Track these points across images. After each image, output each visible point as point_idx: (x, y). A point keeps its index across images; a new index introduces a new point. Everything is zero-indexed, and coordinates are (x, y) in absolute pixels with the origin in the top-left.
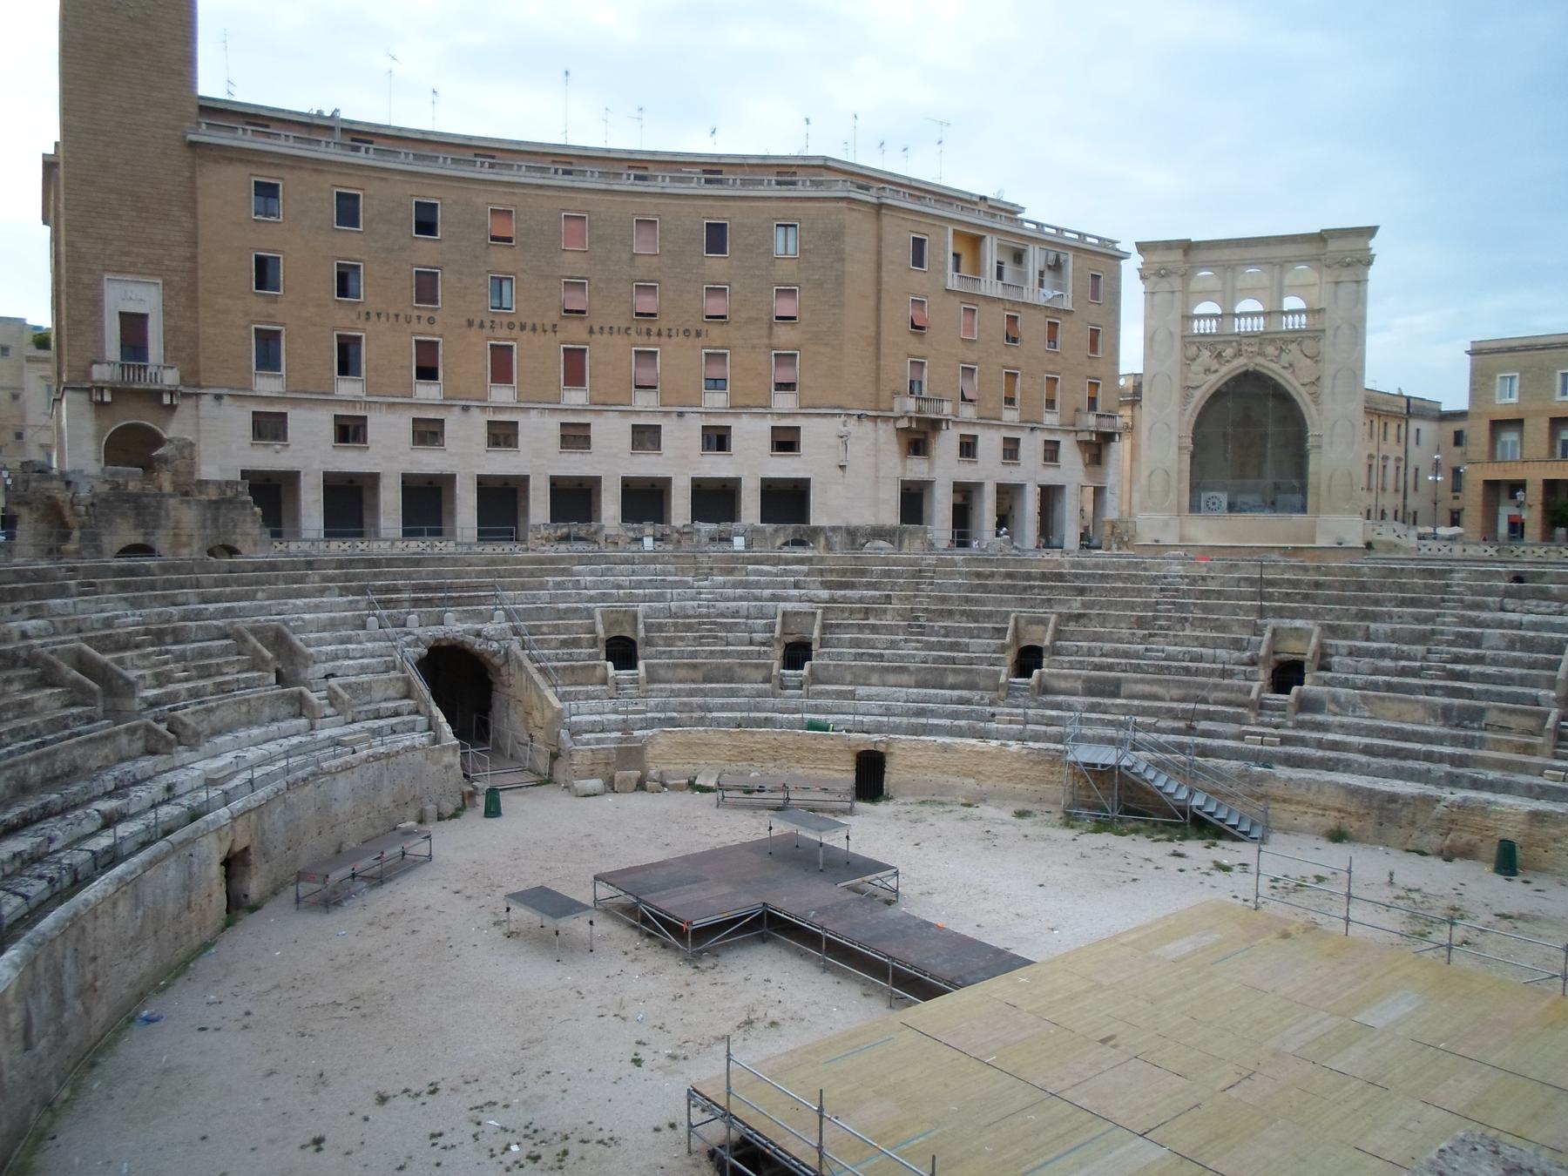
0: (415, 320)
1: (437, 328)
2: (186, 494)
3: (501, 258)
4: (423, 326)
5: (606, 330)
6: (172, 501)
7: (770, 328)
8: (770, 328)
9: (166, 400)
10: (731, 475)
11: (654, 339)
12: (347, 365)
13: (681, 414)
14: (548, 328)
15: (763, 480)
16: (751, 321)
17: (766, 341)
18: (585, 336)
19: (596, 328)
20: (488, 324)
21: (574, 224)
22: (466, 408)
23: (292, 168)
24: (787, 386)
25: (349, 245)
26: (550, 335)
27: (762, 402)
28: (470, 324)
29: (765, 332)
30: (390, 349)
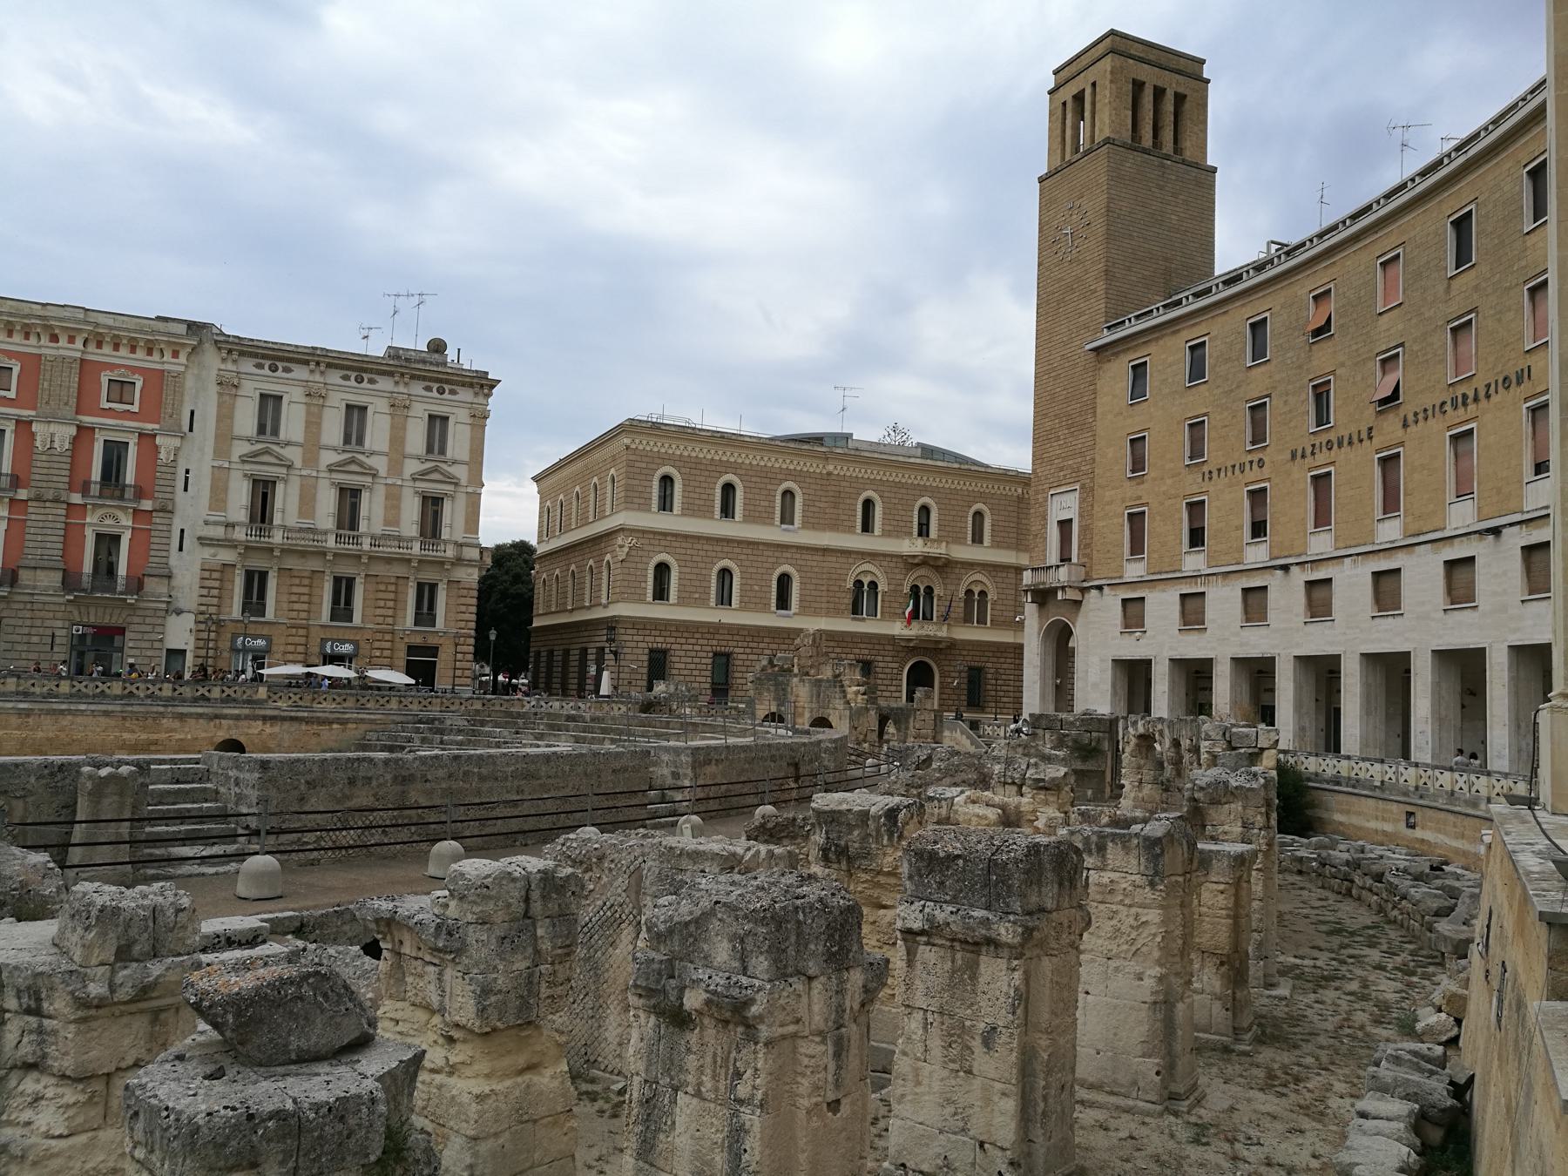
2: (807, 674)
3: (1324, 358)
5: (1421, 416)
6: (795, 680)
9: (1060, 594)
11: (1472, 407)
12: (1197, 537)
13: (1496, 531)
18: (1400, 432)
19: (1411, 418)
21: (1391, 270)
22: (1285, 568)
23: (1157, 339)
25: (1199, 401)
26: (1366, 443)
30: (1227, 510)
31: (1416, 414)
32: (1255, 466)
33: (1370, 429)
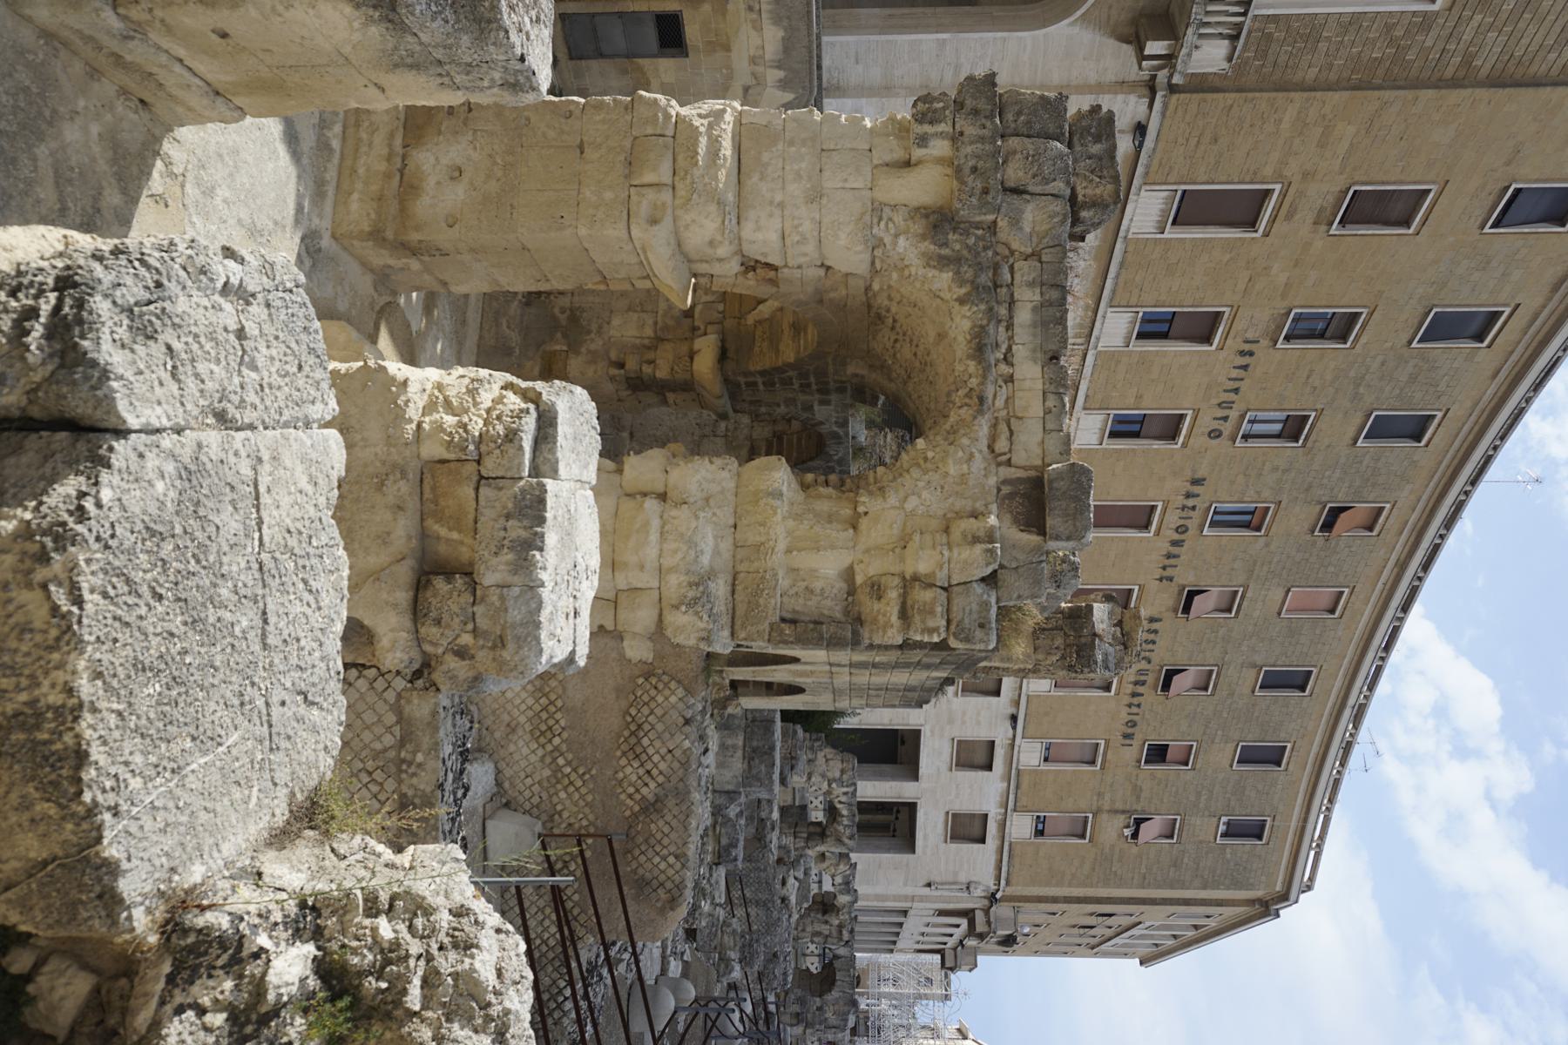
0: (1221, 413)
1: (1200, 441)
4: (1207, 422)
7: (1123, 812)
8: (1123, 812)
10: (921, 771)
13: (1014, 718)
14: (1169, 572)
15: (915, 804)
16: (1137, 791)
17: (1106, 807)
19: (1155, 626)
20: (1190, 502)
24: (1040, 833)
26: (1158, 573)
27: (1023, 801)
28: (1196, 482)
29: (1119, 806)
31: (1156, 632)
32: (1216, 425)
33: (1170, 579)
